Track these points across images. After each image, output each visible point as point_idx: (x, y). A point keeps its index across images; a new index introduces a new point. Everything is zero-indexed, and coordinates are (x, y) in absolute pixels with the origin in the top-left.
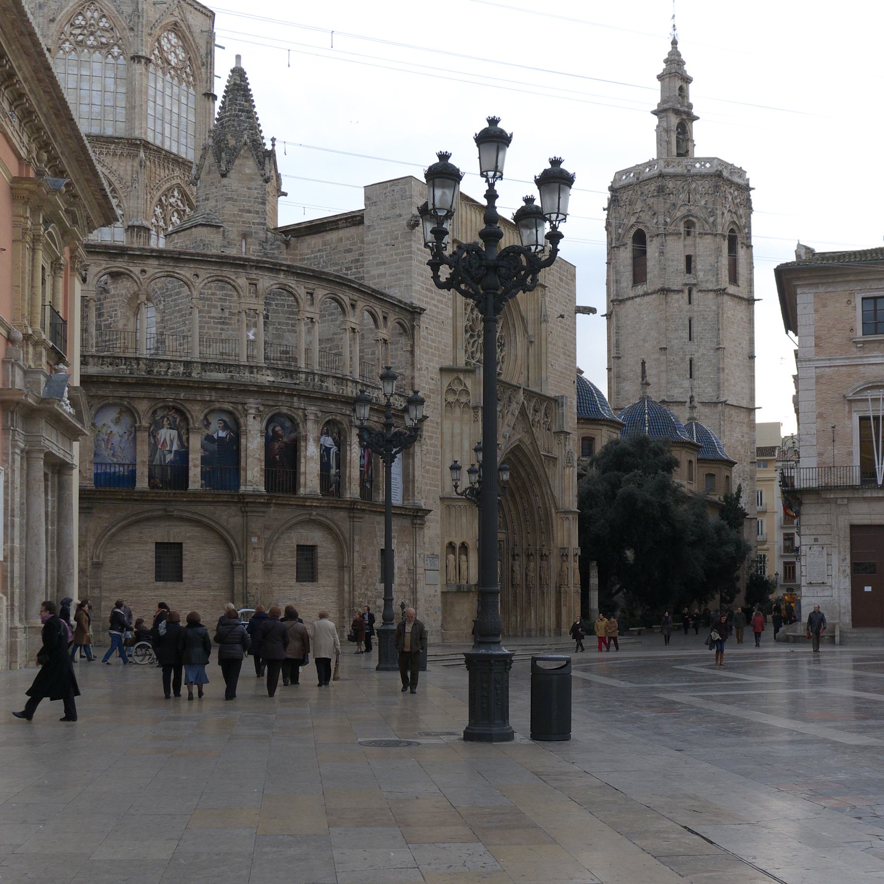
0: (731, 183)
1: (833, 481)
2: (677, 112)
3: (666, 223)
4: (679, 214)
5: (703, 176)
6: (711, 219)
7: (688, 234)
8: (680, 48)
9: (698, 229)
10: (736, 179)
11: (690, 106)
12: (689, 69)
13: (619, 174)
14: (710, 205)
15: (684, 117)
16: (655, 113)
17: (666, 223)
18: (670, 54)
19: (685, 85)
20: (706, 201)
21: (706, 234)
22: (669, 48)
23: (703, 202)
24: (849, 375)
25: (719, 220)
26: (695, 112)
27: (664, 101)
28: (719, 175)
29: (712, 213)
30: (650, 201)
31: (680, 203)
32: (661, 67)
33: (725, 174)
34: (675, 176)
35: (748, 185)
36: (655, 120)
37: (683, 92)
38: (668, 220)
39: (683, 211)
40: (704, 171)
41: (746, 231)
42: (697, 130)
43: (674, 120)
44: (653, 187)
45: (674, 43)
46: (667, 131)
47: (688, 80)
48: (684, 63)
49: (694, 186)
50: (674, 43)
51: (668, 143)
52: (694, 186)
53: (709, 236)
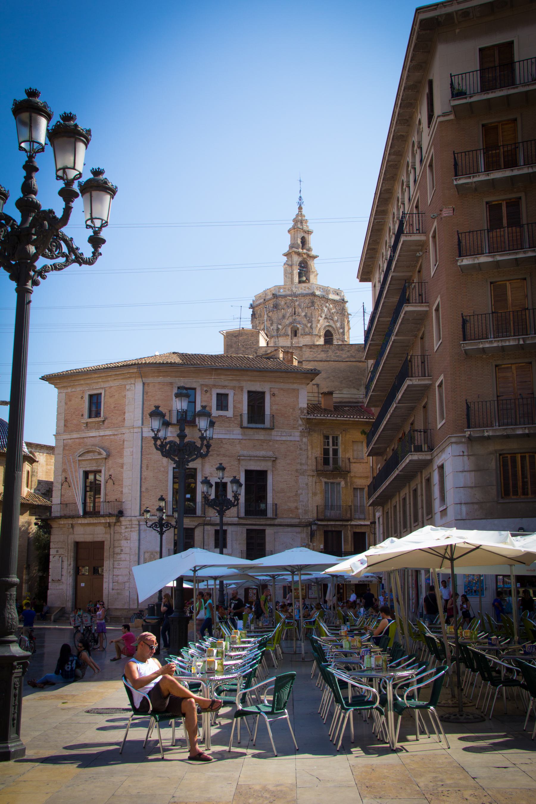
0: (327, 300)
1: (67, 512)
2: (299, 254)
3: (278, 329)
4: (287, 322)
5: (304, 295)
6: (309, 325)
7: (296, 335)
8: (304, 212)
9: (300, 332)
10: (332, 296)
11: (309, 250)
12: (310, 226)
13: (258, 297)
14: (309, 315)
15: (305, 256)
16: (285, 255)
17: (278, 329)
18: (297, 215)
19: (306, 236)
20: (306, 313)
21: (305, 335)
22: (297, 211)
23: (303, 314)
24: (80, 444)
25: (314, 325)
26: (313, 253)
27: (291, 247)
28: (313, 294)
29: (311, 322)
30: (270, 314)
31: (288, 315)
32: (291, 225)
33: (318, 293)
34: (285, 296)
35: (343, 300)
36: (285, 259)
37: (304, 241)
38: (280, 327)
39: (291, 320)
40: (305, 292)
41: (341, 330)
42: (316, 265)
43: (297, 259)
44: (271, 304)
45: (300, 208)
46: (291, 266)
47: (309, 232)
48: (306, 221)
49: (297, 303)
50: (300, 208)
51: (292, 274)
52: (297, 303)
53: (308, 336)
